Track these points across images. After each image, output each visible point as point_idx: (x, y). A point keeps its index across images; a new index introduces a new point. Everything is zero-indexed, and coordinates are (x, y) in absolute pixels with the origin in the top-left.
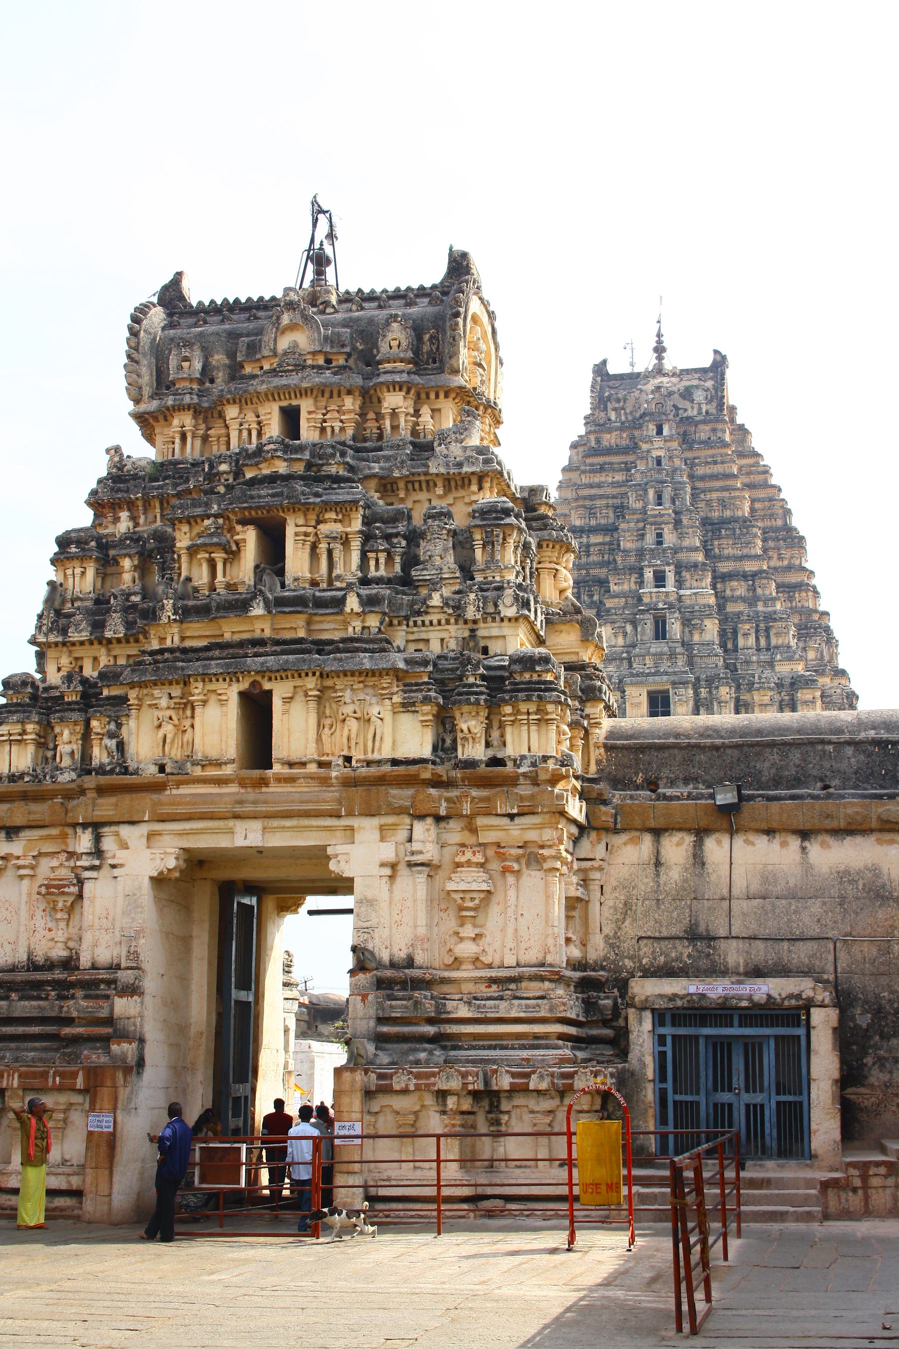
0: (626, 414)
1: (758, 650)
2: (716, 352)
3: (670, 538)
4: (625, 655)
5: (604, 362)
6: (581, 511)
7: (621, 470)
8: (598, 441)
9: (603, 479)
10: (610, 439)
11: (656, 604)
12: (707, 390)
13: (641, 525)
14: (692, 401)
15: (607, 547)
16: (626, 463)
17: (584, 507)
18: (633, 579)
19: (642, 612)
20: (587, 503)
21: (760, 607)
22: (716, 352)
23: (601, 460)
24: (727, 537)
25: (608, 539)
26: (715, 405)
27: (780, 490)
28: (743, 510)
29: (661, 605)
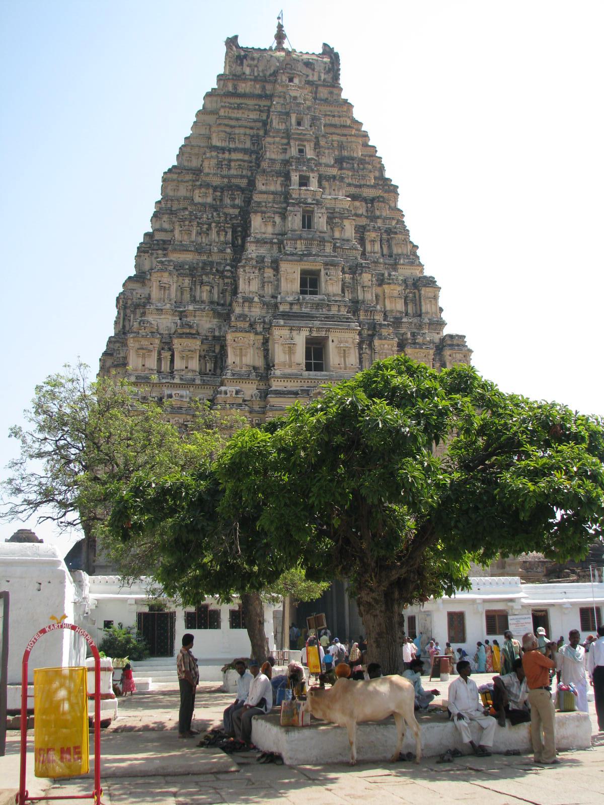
0: (258, 71)
1: (383, 255)
2: (325, 45)
3: (310, 154)
4: (275, 241)
5: (236, 37)
6: (223, 135)
7: (255, 110)
8: (235, 88)
9: (239, 116)
10: (244, 87)
11: (306, 199)
12: (326, 63)
13: (285, 141)
14: (313, 70)
15: (246, 164)
16: (260, 106)
17: (225, 132)
18: (279, 182)
19: (293, 205)
20: (228, 130)
21: (380, 223)
22: (325, 45)
23: (238, 101)
24: (348, 169)
25: (247, 158)
26: (331, 75)
27: (376, 151)
28: (357, 153)
29: (310, 201)
